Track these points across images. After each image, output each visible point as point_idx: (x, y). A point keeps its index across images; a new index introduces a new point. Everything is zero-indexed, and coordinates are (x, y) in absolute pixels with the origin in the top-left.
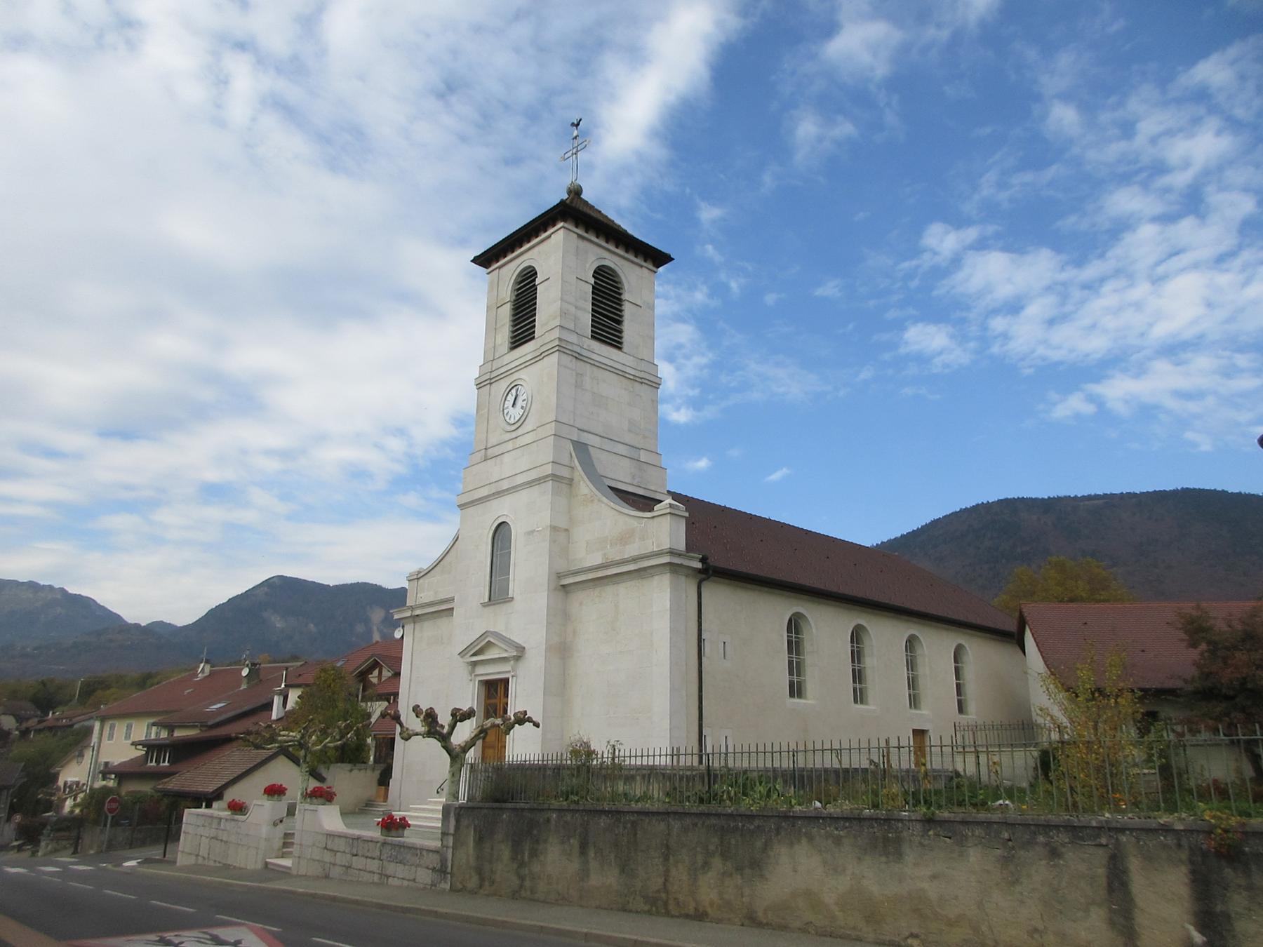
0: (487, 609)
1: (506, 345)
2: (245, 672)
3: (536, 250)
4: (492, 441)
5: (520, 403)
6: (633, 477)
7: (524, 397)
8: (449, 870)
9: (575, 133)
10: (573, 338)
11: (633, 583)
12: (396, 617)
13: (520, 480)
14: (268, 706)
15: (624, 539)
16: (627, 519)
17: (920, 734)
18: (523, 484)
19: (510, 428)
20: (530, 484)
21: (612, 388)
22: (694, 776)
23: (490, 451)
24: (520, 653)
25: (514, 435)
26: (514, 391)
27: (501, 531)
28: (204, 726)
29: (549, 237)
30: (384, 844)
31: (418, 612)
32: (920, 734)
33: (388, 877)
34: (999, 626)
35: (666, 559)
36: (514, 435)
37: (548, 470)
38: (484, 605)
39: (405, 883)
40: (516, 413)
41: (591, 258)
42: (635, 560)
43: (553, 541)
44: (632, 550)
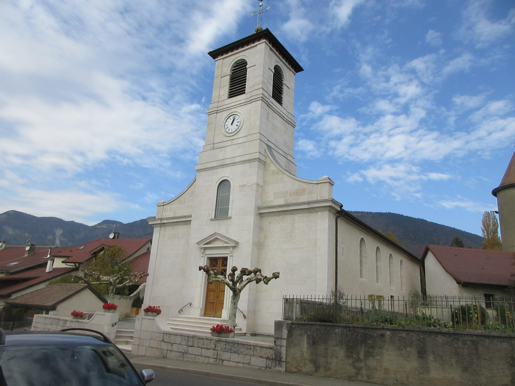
0: (213, 222)
1: (227, 95)
2: (28, 248)
3: (247, 51)
4: (217, 140)
5: (235, 123)
6: (286, 167)
7: (239, 120)
8: (284, 359)
9: (261, 4)
10: (267, 95)
11: (304, 214)
12: (150, 223)
13: (238, 160)
14: (45, 265)
15: (298, 193)
16: (300, 183)
17: (392, 297)
18: (240, 162)
19: (228, 135)
20: (244, 162)
21: (279, 123)
22: (357, 312)
23: (216, 146)
24: (236, 245)
25: (231, 138)
26: (232, 118)
27: (224, 184)
28: (8, 273)
29: (256, 46)
30: (218, 341)
31: (164, 222)
32: (392, 297)
33: (223, 361)
34: (414, 254)
35: (330, 204)
36: (231, 138)
37: (257, 156)
38: (212, 220)
39: (241, 365)
40: (234, 128)
41: (274, 61)
42: (309, 203)
43: (257, 191)
44: (305, 198)
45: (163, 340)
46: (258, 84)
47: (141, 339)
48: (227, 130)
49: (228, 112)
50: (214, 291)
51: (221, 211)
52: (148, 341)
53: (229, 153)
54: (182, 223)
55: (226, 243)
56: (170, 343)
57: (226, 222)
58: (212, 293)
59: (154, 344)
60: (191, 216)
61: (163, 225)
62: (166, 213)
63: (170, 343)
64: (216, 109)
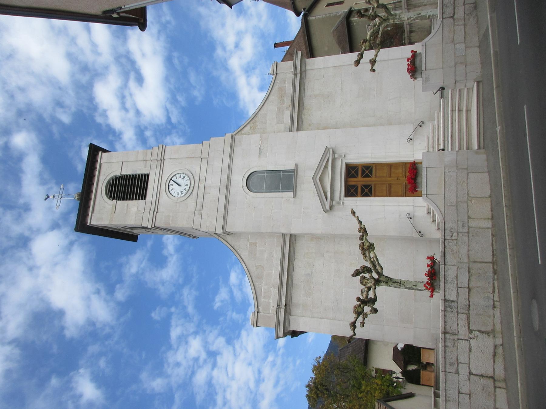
0: (298, 193)
5: (179, 181)
7: (178, 176)
11: (306, 85)
15: (282, 97)
25: (197, 184)
29: (101, 164)
31: (283, 302)
42: (295, 74)
45: (453, 17)
46: (146, 154)
47: (456, 64)
48: (185, 192)
49: (163, 193)
50: (390, 186)
51: (284, 181)
52: (457, 46)
53: (214, 180)
54: (290, 270)
55: (326, 167)
56: (454, 3)
57: (300, 173)
58: (393, 190)
59: (460, 35)
60: (284, 235)
61: (288, 307)
62: (271, 305)
63: (454, 3)
64: (152, 212)
